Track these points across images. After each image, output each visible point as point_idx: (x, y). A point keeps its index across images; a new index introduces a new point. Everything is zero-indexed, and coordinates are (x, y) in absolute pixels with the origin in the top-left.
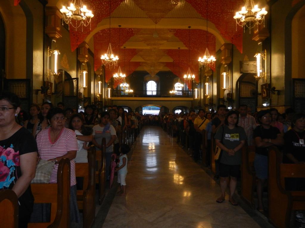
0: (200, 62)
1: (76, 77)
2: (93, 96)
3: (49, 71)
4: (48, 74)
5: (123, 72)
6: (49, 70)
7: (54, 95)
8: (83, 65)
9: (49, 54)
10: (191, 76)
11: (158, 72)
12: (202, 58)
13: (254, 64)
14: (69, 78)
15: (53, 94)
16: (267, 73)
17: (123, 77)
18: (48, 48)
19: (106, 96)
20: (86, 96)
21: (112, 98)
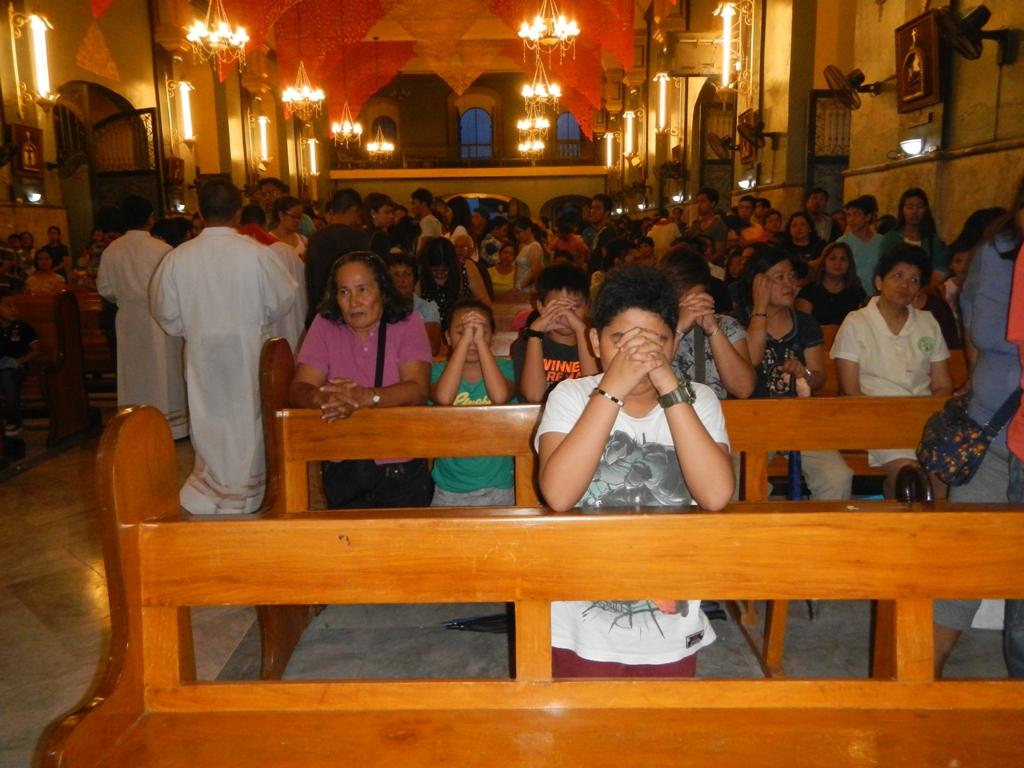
0: (525, 41)
1: (154, 105)
2: (243, 167)
3: (22, 89)
4: (20, 103)
5: (315, 82)
6: (21, 84)
7: (56, 170)
8: (178, 61)
9: (15, 29)
10: (546, 88)
11: (477, 76)
12: (531, 24)
13: (716, 41)
14: (129, 114)
15: (50, 166)
16: (754, 73)
17: (316, 100)
18: (8, 5)
19: (301, 167)
20: (213, 167)
21: (332, 172)
